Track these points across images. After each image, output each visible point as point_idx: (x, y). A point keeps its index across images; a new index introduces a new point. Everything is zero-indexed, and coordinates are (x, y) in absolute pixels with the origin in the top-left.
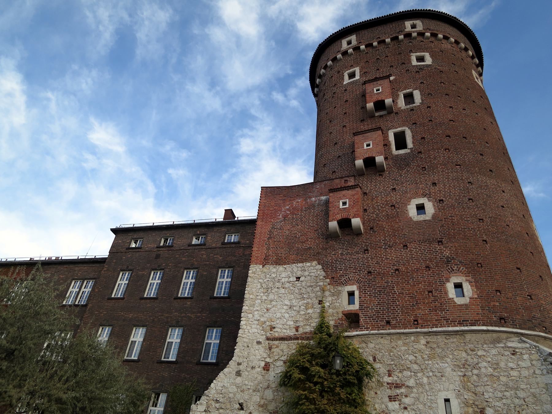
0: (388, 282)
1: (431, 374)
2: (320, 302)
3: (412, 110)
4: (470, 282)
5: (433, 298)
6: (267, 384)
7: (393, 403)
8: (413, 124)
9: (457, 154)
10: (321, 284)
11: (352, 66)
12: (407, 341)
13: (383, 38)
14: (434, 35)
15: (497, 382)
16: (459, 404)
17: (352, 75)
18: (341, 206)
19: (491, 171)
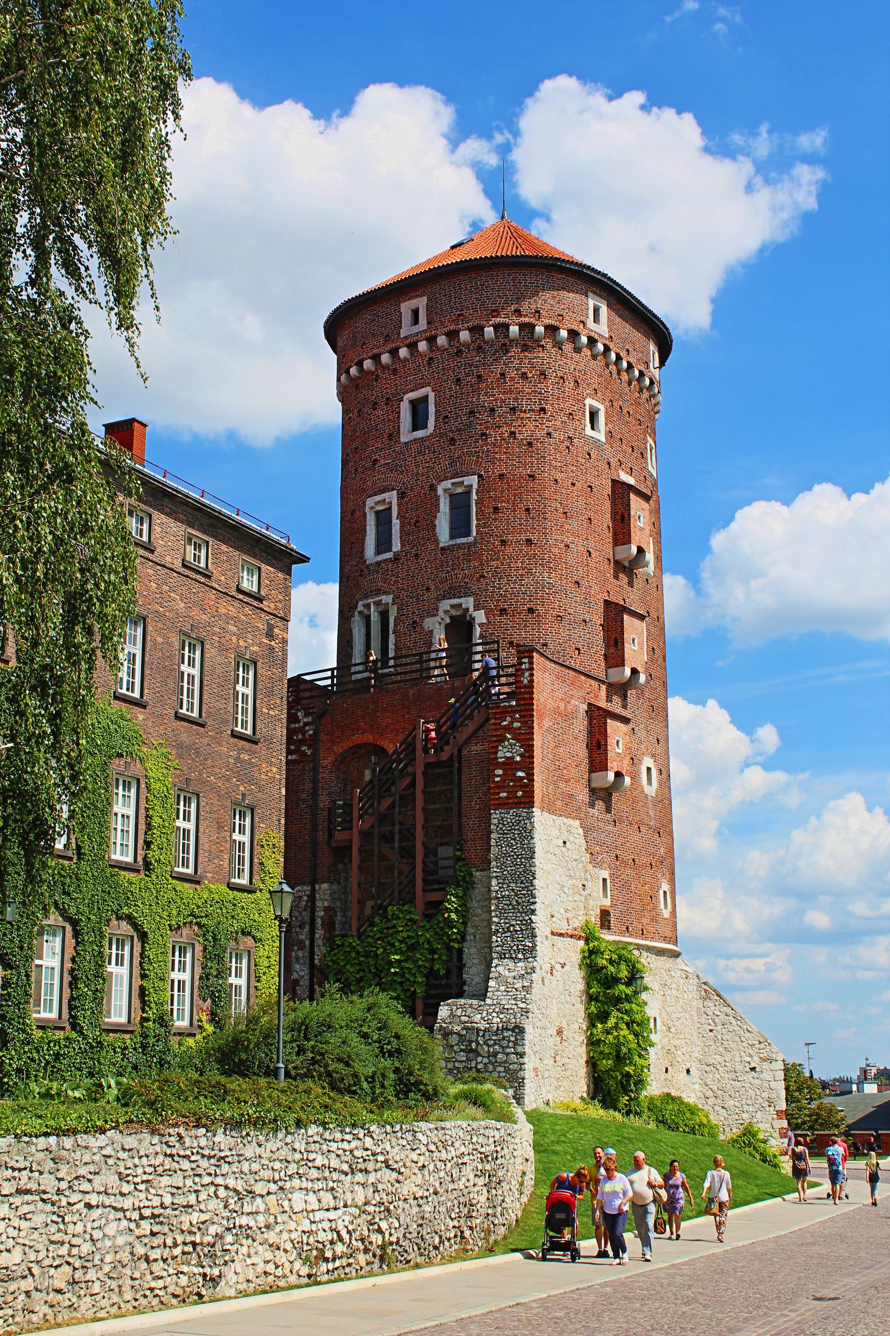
13: (631, 360)
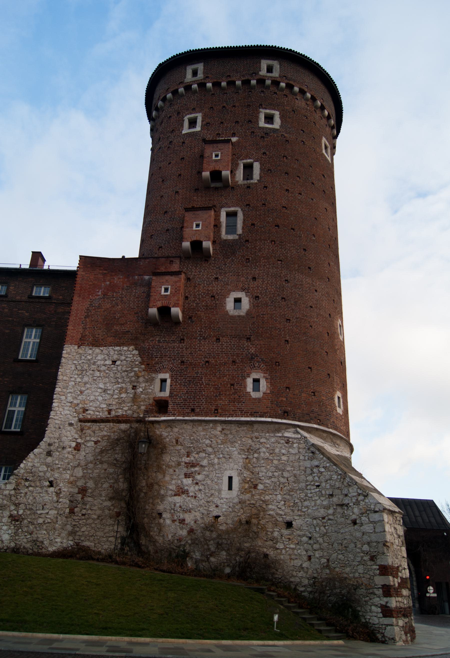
0: (197, 373)
1: (221, 456)
2: (134, 388)
3: (249, 187)
4: (267, 379)
5: (233, 391)
6: (77, 463)
7: (188, 479)
8: (247, 205)
9: (281, 248)
10: (136, 369)
11: (194, 109)
12: (207, 427)
14: (290, 87)
15: (270, 465)
16: (239, 480)
17: (193, 123)
18: (163, 293)
19: (309, 268)
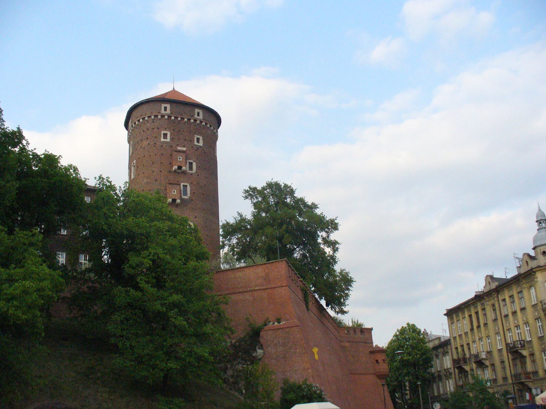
17: (165, 135)
